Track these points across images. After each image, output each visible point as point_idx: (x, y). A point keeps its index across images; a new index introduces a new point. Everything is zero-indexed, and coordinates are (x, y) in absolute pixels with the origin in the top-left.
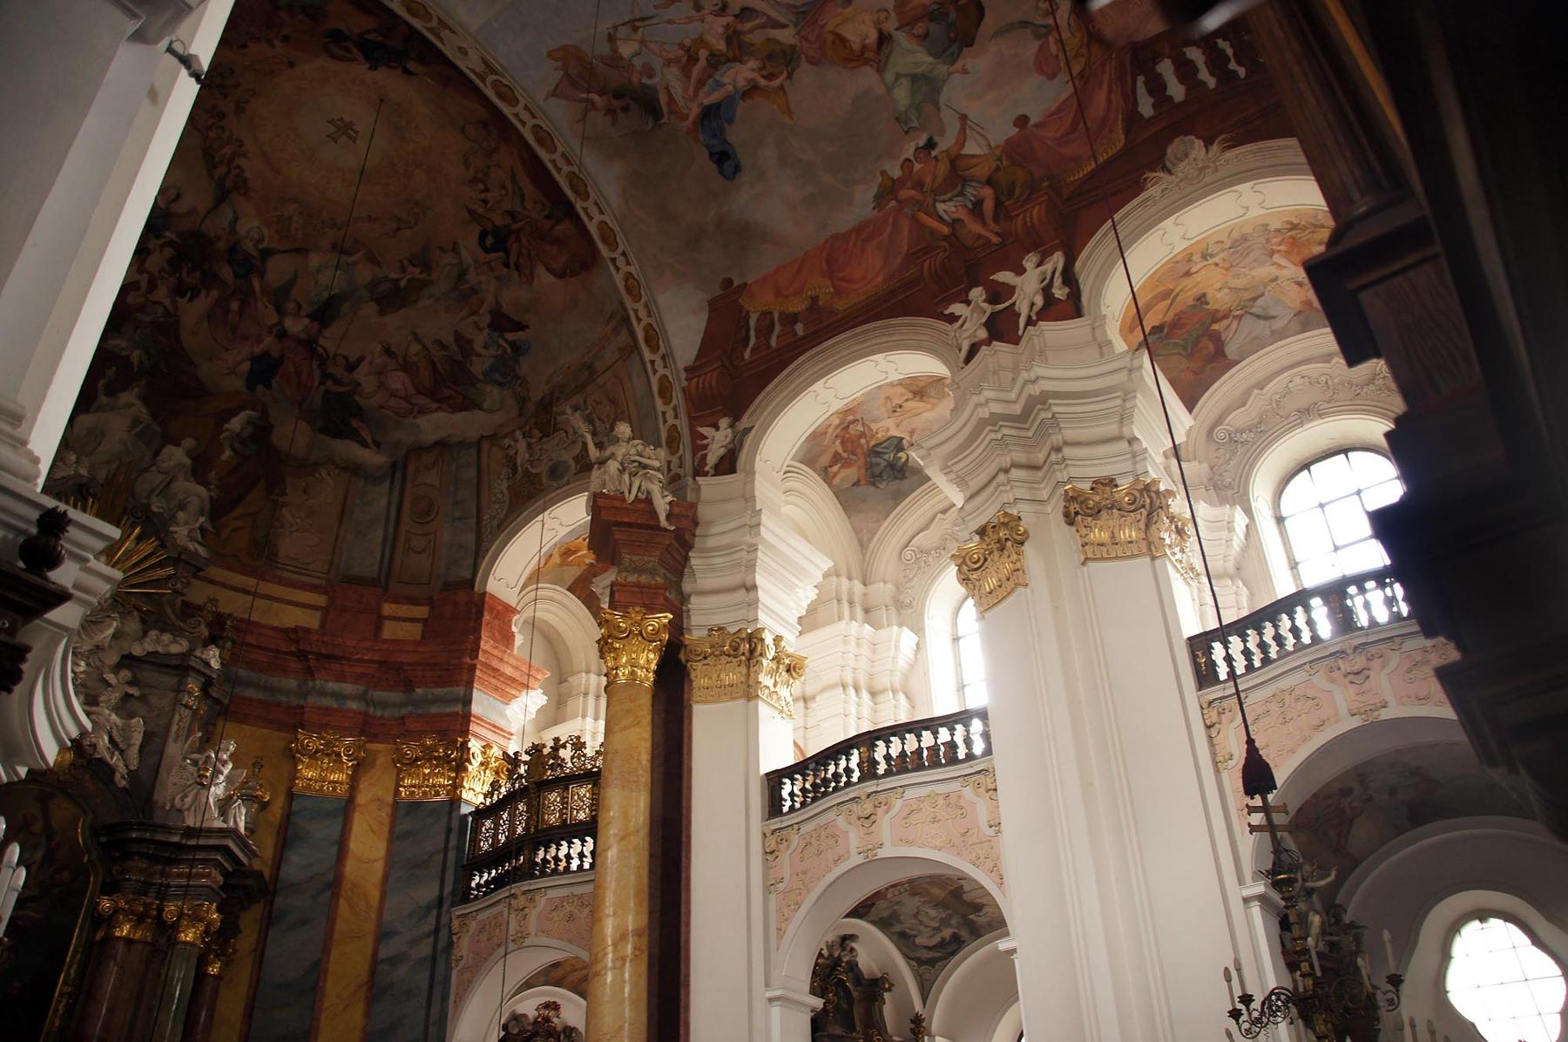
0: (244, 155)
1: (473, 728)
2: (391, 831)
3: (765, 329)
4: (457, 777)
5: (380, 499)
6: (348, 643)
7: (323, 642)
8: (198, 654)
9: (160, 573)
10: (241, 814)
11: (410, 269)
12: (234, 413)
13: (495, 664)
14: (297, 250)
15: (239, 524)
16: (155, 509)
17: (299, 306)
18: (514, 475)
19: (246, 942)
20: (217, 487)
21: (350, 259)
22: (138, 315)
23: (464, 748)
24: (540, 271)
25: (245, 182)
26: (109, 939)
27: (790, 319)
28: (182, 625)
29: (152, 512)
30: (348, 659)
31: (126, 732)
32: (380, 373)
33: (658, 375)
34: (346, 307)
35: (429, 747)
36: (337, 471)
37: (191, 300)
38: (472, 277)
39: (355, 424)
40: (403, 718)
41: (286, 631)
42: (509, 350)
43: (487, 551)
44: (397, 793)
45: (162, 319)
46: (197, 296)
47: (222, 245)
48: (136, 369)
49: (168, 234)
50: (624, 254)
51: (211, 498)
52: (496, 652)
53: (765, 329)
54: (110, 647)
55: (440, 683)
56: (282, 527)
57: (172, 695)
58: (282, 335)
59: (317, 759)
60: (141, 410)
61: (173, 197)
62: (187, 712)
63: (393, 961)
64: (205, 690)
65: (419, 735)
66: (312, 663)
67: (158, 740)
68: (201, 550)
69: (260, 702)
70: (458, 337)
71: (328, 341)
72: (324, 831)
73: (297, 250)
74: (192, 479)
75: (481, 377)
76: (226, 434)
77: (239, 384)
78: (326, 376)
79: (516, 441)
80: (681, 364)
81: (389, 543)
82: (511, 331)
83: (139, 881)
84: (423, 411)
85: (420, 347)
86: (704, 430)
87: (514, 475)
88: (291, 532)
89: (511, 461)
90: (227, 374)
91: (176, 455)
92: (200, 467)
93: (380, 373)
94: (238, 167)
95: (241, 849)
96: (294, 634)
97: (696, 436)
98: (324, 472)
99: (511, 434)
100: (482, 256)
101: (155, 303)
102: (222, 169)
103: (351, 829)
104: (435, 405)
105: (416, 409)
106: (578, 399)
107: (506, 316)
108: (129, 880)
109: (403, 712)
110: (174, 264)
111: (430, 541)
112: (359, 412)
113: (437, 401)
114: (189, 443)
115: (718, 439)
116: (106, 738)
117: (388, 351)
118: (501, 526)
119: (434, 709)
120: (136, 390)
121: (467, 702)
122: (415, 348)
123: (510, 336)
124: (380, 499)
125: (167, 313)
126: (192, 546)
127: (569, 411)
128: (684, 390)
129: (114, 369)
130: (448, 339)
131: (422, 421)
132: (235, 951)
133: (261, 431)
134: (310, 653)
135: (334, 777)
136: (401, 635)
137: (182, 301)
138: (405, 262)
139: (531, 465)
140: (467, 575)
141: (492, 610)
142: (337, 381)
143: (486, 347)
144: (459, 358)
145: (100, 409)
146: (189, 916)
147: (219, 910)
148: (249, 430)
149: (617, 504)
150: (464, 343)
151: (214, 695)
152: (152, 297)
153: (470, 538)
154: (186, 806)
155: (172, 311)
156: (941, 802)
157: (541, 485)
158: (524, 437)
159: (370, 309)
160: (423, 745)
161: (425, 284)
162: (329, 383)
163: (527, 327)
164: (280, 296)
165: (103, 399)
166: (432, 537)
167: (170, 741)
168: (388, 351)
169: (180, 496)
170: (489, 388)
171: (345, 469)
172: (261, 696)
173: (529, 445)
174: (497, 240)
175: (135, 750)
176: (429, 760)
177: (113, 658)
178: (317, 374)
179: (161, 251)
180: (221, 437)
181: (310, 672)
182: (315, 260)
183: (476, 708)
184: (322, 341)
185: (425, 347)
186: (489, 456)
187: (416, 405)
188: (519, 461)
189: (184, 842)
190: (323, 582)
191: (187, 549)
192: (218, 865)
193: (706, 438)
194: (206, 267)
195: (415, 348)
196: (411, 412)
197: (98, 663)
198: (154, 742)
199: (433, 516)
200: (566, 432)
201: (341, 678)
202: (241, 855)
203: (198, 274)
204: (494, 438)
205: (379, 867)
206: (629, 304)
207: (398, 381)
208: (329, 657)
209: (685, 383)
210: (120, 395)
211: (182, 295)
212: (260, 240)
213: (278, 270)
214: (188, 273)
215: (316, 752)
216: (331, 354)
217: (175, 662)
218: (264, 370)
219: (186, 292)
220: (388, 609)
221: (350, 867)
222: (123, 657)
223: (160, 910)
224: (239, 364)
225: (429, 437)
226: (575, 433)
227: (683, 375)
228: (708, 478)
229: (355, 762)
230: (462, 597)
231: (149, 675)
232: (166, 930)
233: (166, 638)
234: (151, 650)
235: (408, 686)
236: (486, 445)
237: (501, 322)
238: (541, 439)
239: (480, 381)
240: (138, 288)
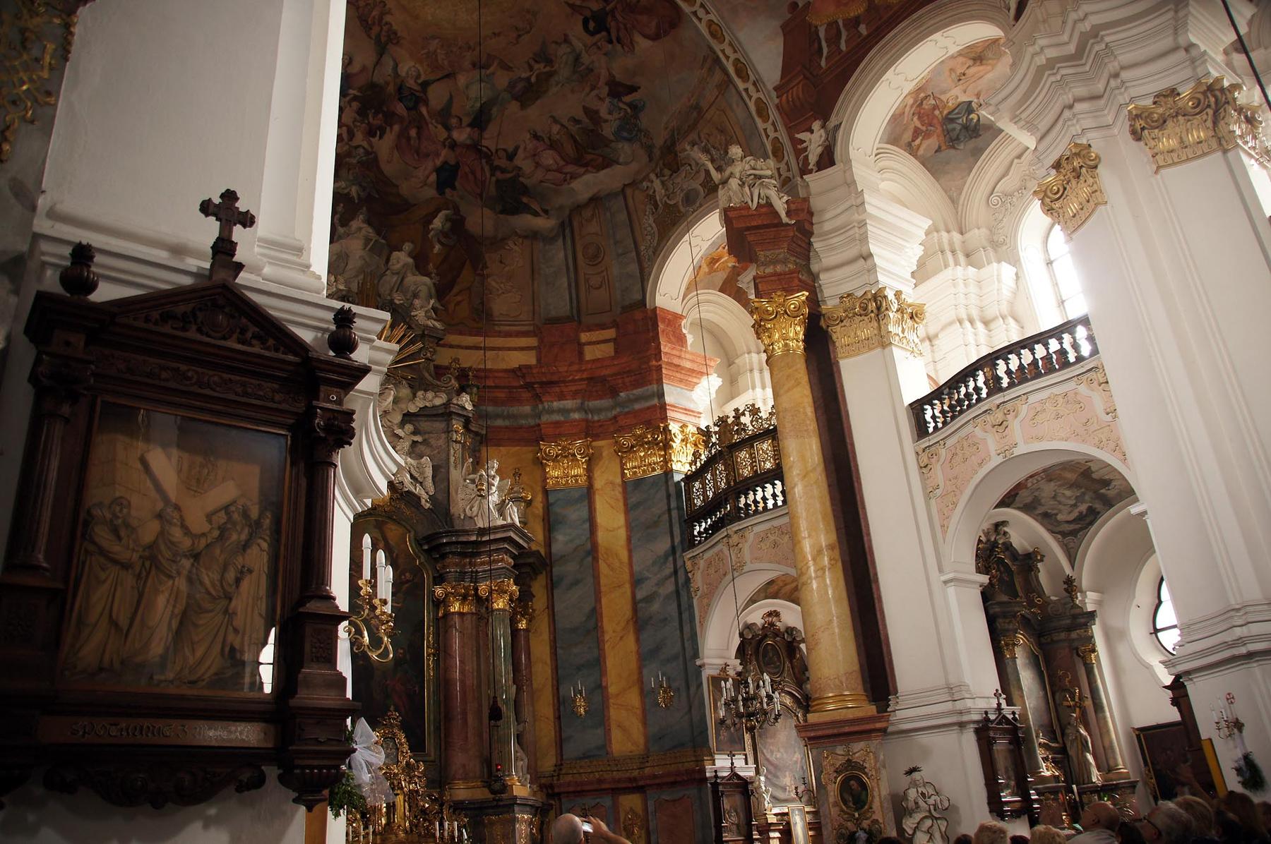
0: (389, 12)
1: (670, 414)
2: (626, 504)
3: (834, 39)
4: (666, 454)
5: (558, 254)
6: (561, 369)
7: (542, 373)
8: (455, 402)
9: (414, 348)
10: (514, 512)
11: (536, 66)
12: (434, 215)
13: (676, 361)
14: (448, 76)
15: (459, 298)
16: (397, 302)
17: (461, 120)
18: (656, 209)
19: (539, 603)
20: (437, 274)
21: (488, 72)
23: (666, 430)
24: (639, 39)
25: (395, 33)
26: (447, 615)
27: (854, 23)
28: (439, 383)
29: (395, 304)
30: (564, 382)
31: (420, 468)
32: (535, 155)
33: (753, 99)
34: (494, 110)
35: (640, 436)
36: (520, 240)
37: (381, 137)
38: (586, 59)
39: (525, 200)
40: (615, 417)
41: (513, 371)
42: (629, 110)
43: (650, 275)
44: (623, 475)
45: (364, 158)
46: (385, 133)
47: (391, 89)
48: (356, 201)
49: (351, 91)
50: (702, 6)
51: (434, 284)
52: (674, 352)
53: (834, 39)
54: (393, 409)
55: (638, 384)
57: (444, 436)
58: (453, 145)
59: (558, 461)
60: (368, 231)
62: (458, 446)
63: (649, 599)
64: (466, 426)
65: (630, 428)
66: (538, 391)
67: (443, 470)
68: (438, 325)
69: (507, 427)
70: (587, 110)
71: (488, 142)
72: (576, 514)
73: (448, 76)
75: (612, 137)
76: (432, 233)
77: (431, 192)
78: (494, 169)
79: (652, 182)
80: (770, 86)
81: (573, 285)
82: (627, 95)
83: (457, 572)
84: (574, 177)
85: (559, 126)
86: (801, 136)
87: (656, 209)
88: (499, 295)
89: (652, 198)
90: (421, 187)
91: (401, 258)
92: (420, 263)
93: (535, 155)
94: (387, 23)
95: (521, 538)
96: (520, 371)
97: (796, 142)
98: (511, 243)
99: (646, 178)
100: (589, 40)
102: (376, 29)
103: (595, 508)
104: (583, 170)
105: (568, 176)
106: (693, 136)
107: (619, 84)
108: (450, 572)
109: (614, 413)
111: (604, 277)
112: (525, 190)
113: (586, 165)
114: (408, 246)
115: (814, 140)
116: (408, 476)
117: (536, 137)
118: (656, 252)
119: (637, 406)
120: (361, 217)
121: (661, 395)
122: (556, 128)
123: (627, 99)
124: (558, 254)
125: (367, 153)
126: (430, 323)
127: (688, 148)
128: (777, 107)
130: (580, 115)
131: (576, 185)
132: (534, 610)
133: (457, 224)
134: (534, 383)
135: (575, 472)
136: (599, 355)
137: (375, 140)
138: (532, 62)
139: (668, 198)
140: (638, 297)
141: (664, 320)
142: (503, 171)
143: (610, 113)
144: (592, 127)
146: (496, 591)
147: (516, 584)
148: (448, 225)
149: (744, 213)
150: (592, 114)
151: (473, 429)
152: (354, 143)
153: (634, 268)
154: (475, 514)
155: (370, 150)
156: (1061, 400)
157: (679, 211)
158: (657, 177)
159: (514, 106)
160: (634, 435)
161: (550, 75)
162: (498, 173)
163: (639, 88)
164: (444, 116)
166: (605, 273)
167: (452, 469)
168: (536, 137)
169: (412, 288)
170: (620, 145)
171: (526, 237)
172: (507, 423)
173: (663, 183)
174: (597, 23)
175: (430, 480)
176: (642, 445)
177: (397, 418)
178: (487, 168)
180: (430, 236)
181: (538, 398)
182: (462, 80)
183: (669, 399)
184: (484, 143)
185: (562, 125)
186: (633, 198)
187: (566, 174)
188: (658, 198)
190: (531, 328)
191: (427, 327)
192: (507, 551)
193: (805, 142)
194: (385, 109)
195: (556, 128)
196: (565, 180)
197: (389, 424)
198: (440, 473)
199: (600, 259)
200: (690, 165)
201: (562, 397)
202: (521, 542)
203: (380, 116)
204: (634, 184)
205: (622, 533)
206: (717, 47)
207: (549, 158)
208: (551, 383)
209: (777, 101)
210: (352, 223)
211: (374, 136)
212: (418, 76)
213: (437, 95)
215: (557, 456)
216: (493, 150)
217: (440, 412)
218: (447, 177)
219: (376, 133)
220: (584, 337)
221: (601, 536)
222: (404, 415)
223: (476, 589)
225: (584, 195)
226: (697, 164)
227: (774, 94)
228: (814, 174)
229: (587, 458)
230: (638, 315)
231: (424, 425)
232: (483, 603)
233: (430, 395)
235: (614, 392)
236: (629, 192)
237: (618, 89)
238: (671, 175)
239: (613, 141)
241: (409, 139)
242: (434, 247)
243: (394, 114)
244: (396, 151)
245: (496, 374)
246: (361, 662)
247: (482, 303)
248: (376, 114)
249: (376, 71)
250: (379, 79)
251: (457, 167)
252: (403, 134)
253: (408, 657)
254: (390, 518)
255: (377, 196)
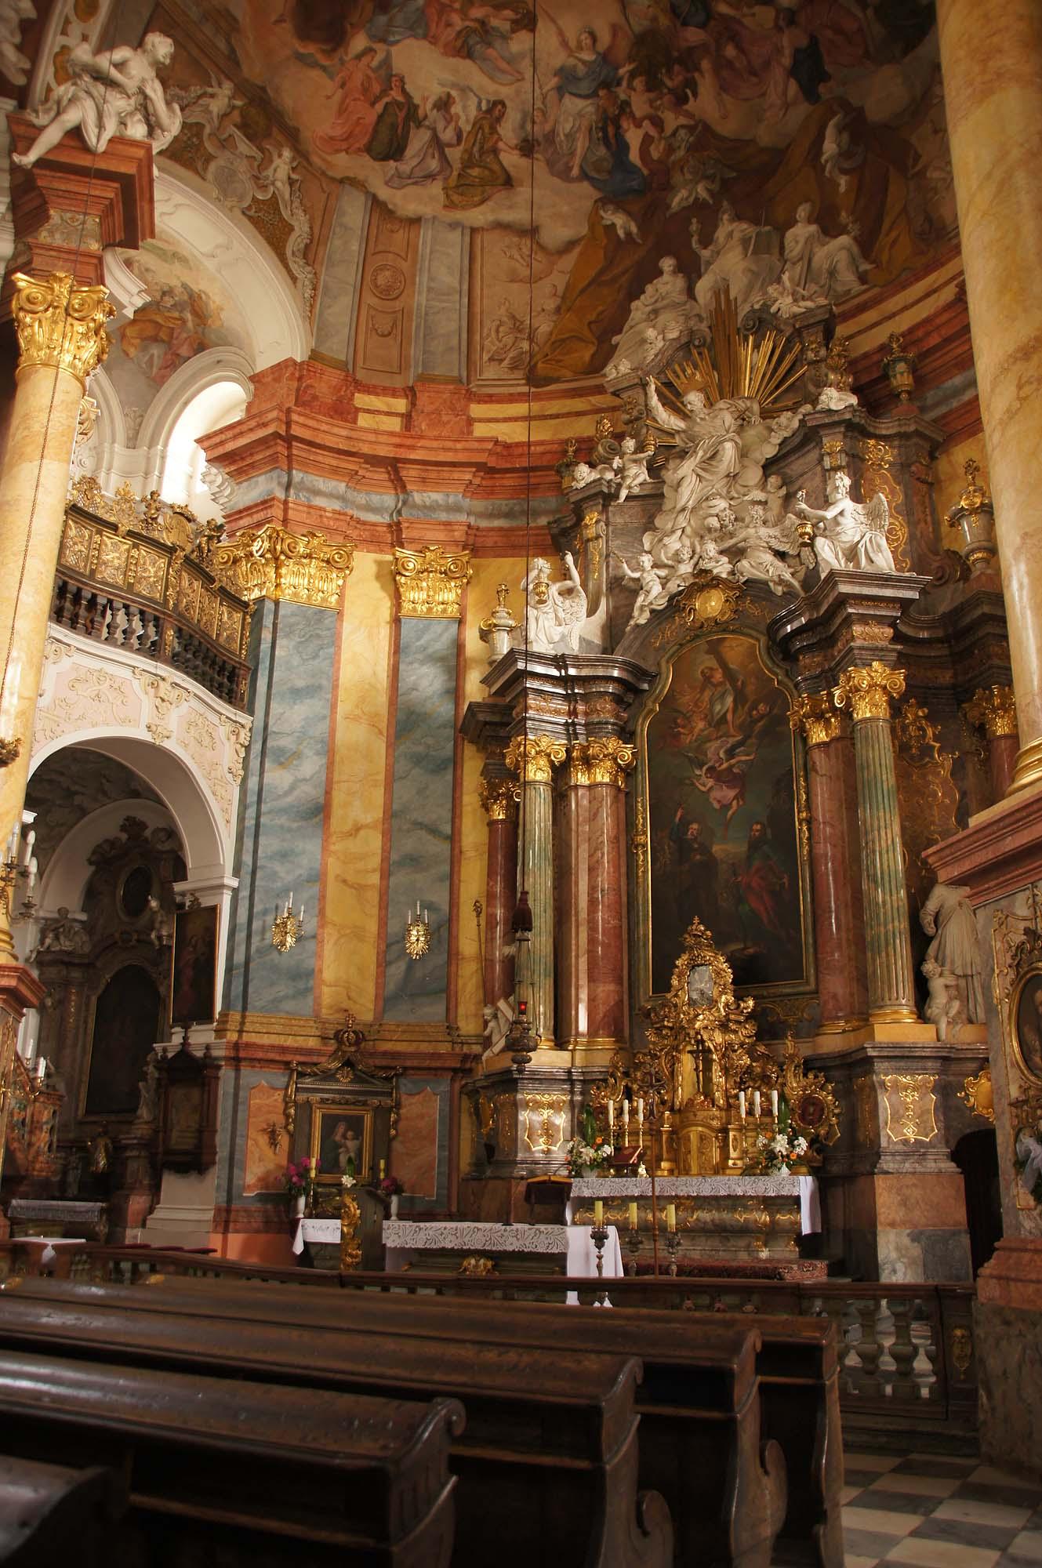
12: (820, 138)
15: (894, 234)
22: (673, 158)
37: (695, 95)
45: (691, 139)
46: (696, 84)
47: (664, 21)
48: (711, 202)
49: (622, 71)
51: (855, 239)
56: (936, 194)
60: (743, 228)
61: (589, 41)
74: (827, 239)
76: (828, 166)
77: (803, 109)
90: (785, 114)
91: (800, 233)
101: (674, 134)
110: (653, 86)
114: (802, 212)
120: (726, 217)
125: (691, 129)
129: (694, 220)
137: (691, 106)
145: (709, 263)
148: (845, 136)
152: (668, 131)
155: (692, 123)
165: (705, 254)
169: (826, 266)
177: (754, 475)
179: (635, 90)
180: (827, 174)
189: (815, 616)
191: (795, 316)
194: (676, 54)
203: (676, 68)
210: (716, 235)
211: (686, 100)
214: (671, 79)
219: (686, 94)
222: (764, 467)
223: (831, 695)
224: (785, 93)
231: (796, 466)
234: (779, 441)
240: (653, 138)
241: (730, 64)
242: (839, 185)
243: (691, 50)
244: (725, 96)
245: (938, 321)
246: (698, 857)
247: (929, 219)
248: (669, 72)
249: (631, 21)
250: (639, 25)
251: (814, 41)
252: (722, 65)
253: (769, 836)
254: (724, 630)
255: (734, 174)
